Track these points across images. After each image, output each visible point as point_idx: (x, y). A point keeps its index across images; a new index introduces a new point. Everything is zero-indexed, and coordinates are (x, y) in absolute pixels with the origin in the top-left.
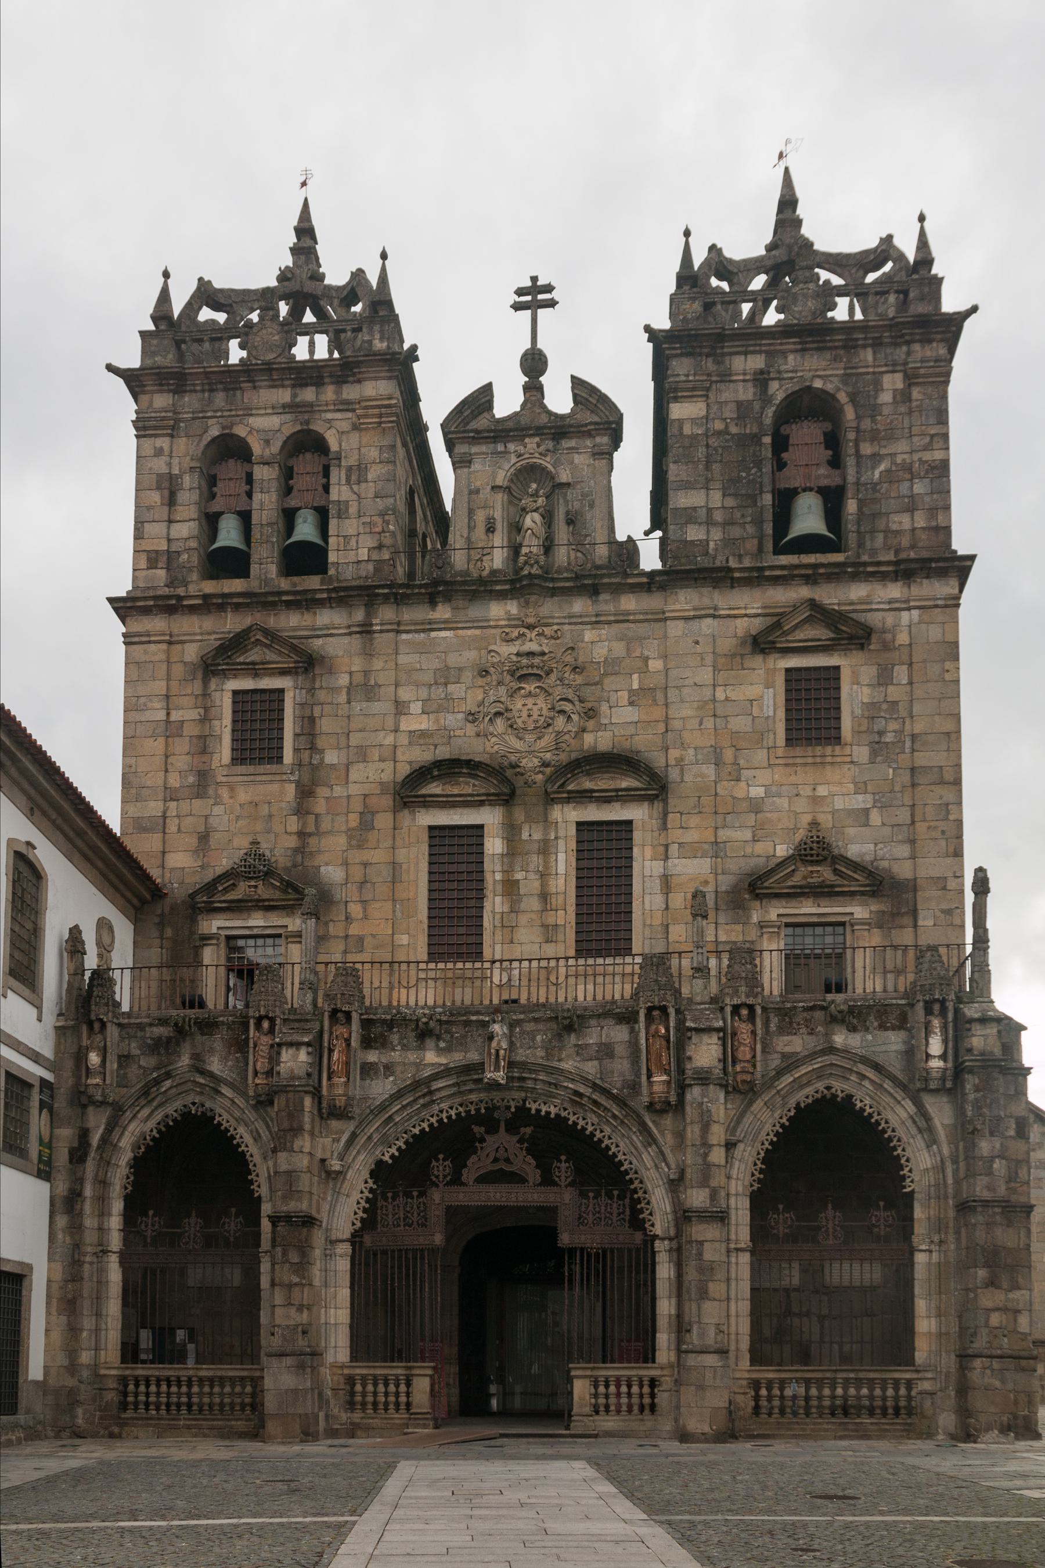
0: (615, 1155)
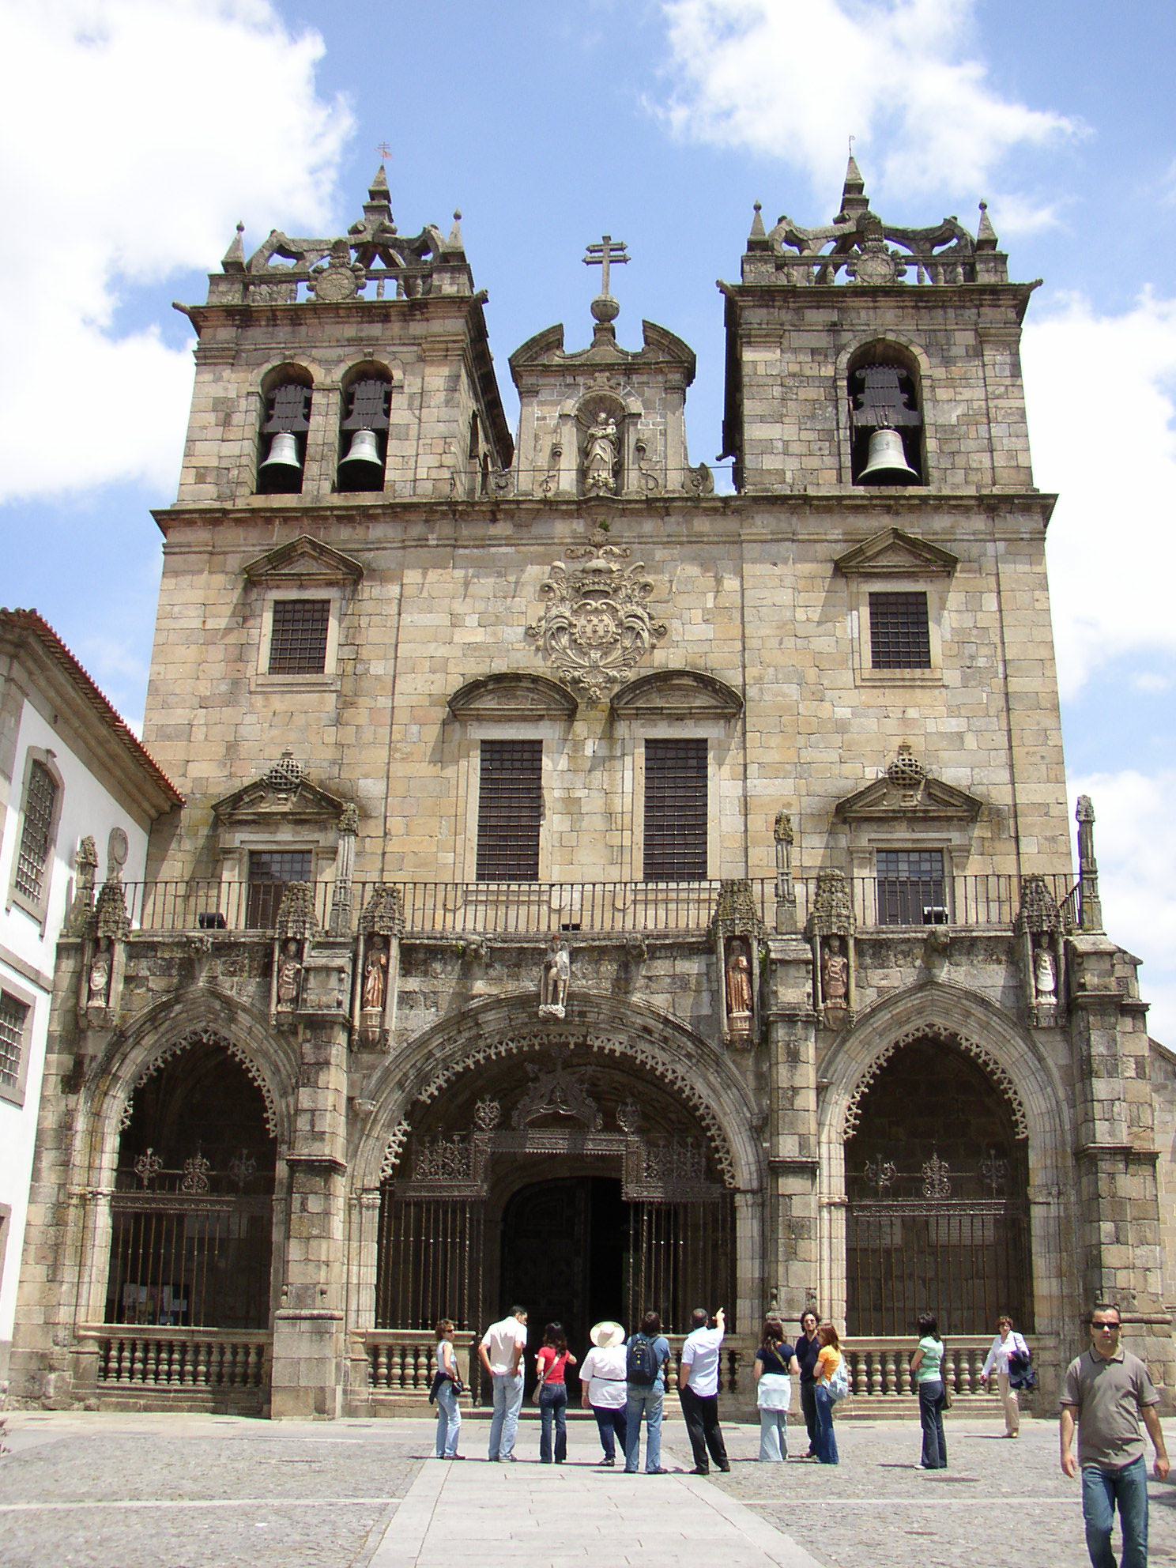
0: (689, 1098)
